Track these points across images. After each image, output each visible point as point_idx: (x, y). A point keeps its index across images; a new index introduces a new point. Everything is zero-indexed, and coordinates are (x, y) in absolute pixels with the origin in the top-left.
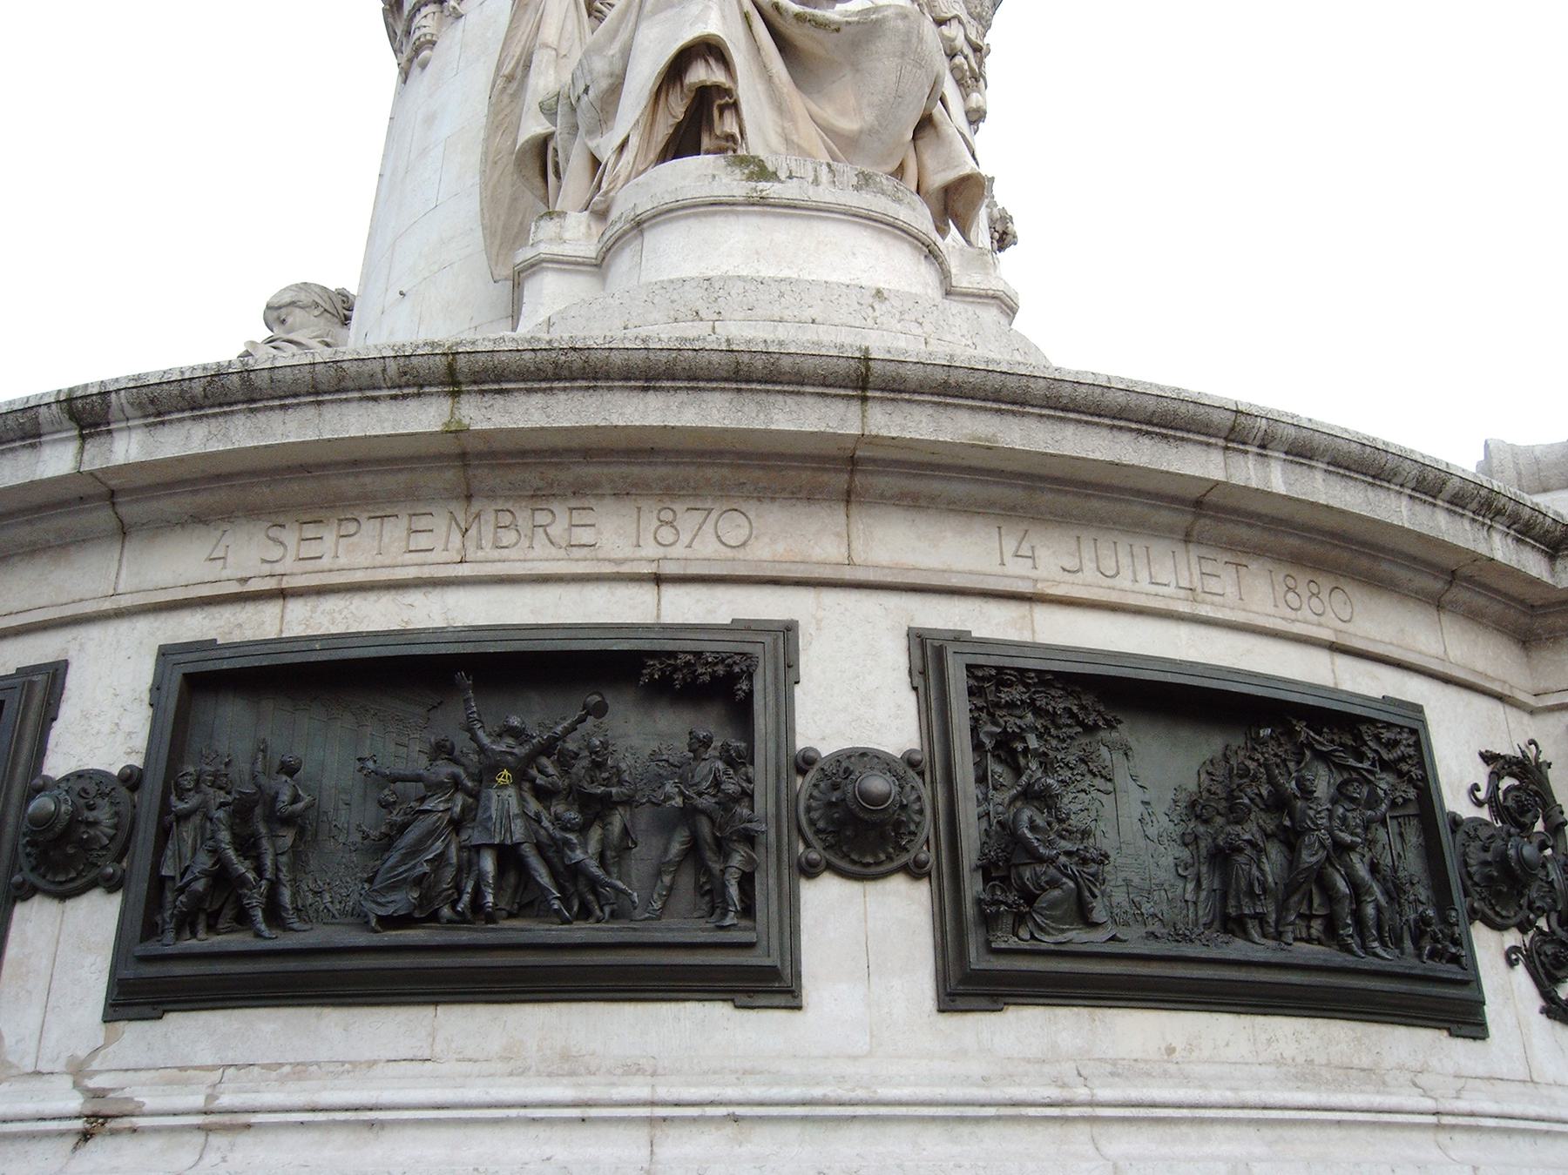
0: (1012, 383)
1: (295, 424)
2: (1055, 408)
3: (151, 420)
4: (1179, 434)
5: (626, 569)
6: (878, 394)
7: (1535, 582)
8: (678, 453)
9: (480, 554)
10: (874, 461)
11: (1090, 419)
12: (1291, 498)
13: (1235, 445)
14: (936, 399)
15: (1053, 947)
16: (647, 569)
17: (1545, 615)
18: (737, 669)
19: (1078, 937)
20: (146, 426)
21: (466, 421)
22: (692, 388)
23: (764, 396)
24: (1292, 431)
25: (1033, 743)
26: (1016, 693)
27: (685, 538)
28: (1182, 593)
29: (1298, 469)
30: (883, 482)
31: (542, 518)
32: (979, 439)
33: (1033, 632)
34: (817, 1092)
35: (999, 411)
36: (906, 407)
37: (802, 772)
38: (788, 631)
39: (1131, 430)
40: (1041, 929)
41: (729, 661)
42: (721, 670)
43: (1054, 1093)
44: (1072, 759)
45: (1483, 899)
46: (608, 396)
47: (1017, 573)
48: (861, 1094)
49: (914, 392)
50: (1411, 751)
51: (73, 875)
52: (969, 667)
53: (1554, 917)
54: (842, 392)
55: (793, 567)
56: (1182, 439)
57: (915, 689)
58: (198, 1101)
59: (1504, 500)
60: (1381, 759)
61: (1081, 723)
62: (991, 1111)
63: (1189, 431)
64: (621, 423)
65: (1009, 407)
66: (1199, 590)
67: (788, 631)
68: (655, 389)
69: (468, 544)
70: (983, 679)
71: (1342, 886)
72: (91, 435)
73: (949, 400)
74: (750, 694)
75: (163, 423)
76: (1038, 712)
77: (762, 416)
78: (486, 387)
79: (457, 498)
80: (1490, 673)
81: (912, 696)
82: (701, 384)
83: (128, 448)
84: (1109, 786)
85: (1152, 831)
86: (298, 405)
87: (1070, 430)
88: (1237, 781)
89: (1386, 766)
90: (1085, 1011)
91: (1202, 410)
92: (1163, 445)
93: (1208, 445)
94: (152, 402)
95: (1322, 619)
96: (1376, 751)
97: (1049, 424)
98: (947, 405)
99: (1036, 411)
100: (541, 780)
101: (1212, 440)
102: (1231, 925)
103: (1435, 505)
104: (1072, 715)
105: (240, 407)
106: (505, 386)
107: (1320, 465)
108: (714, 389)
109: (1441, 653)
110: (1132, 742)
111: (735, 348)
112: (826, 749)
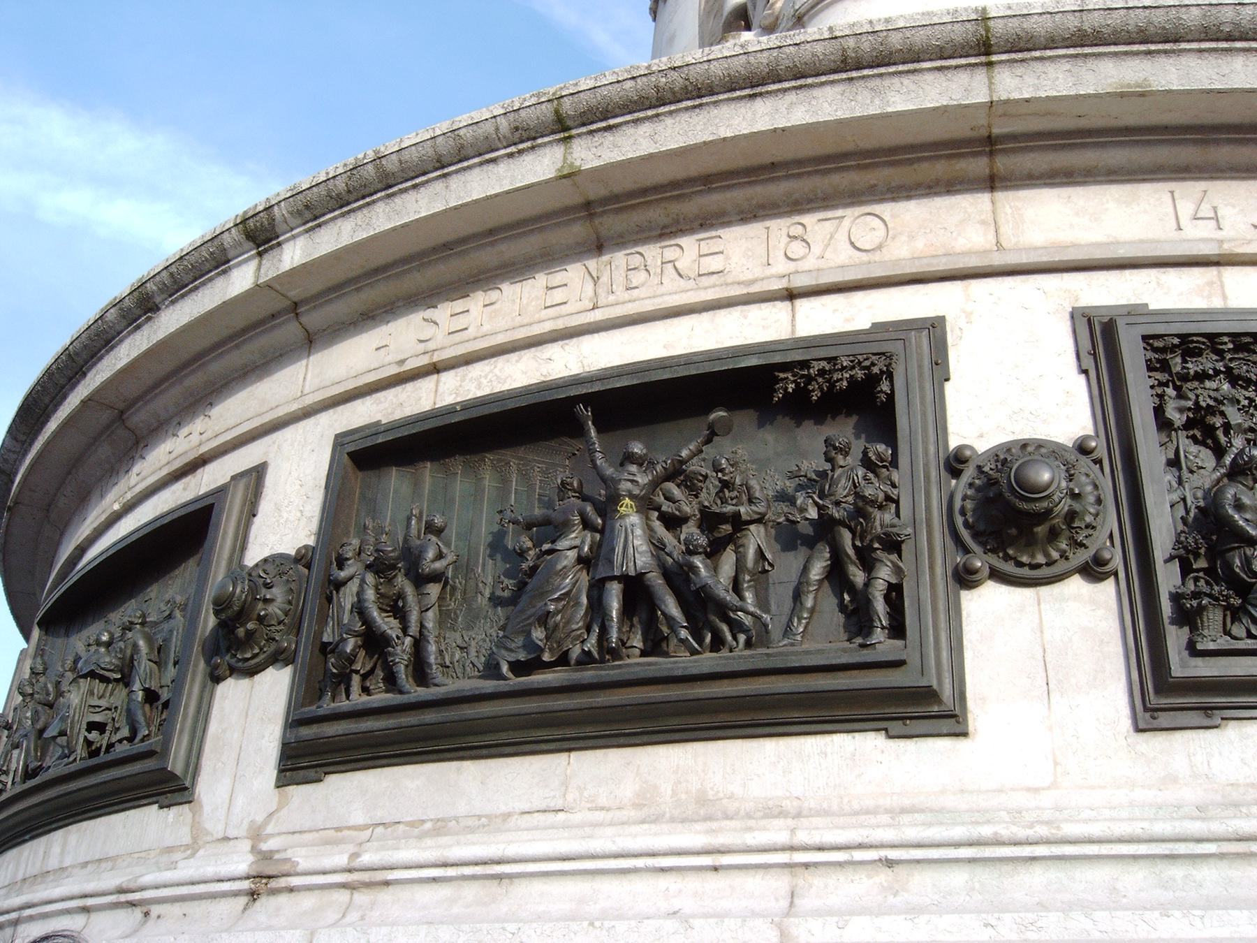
0: (1159, 18)
1: (426, 200)
2: (1218, 40)
3: (310, 224)
6: (1004, 57)
8: (799, 163)
9: (612, 298)
10: (1014, 137)
14: (1072, 51)
18: (876, 370)
20: (307, 231)
21: (577, 163)
22: (800, 87)
23: (878, 81)
26: (1208, 362)
27: (816, 249)
31: (670, 254)
32: (1129, 85)
33: (1225, 297)
35: (1149, 53)
36: (1038, 66)
37: (956, 473)
38: (934, 328)
41: (867, 363)
42: (859, 374)
46: (715, 111)
47: (1199, 237)
48: (1043, 831)
49: (1045, 48)
51: (256, 651)
52: (1145, 338)
54: (963, 61)
55: (935, 261)
57: (1085, 372)
58: (341, 860)
64: (729, 134)
65: (1160, 47)
67: (934, 328)
68: (761, 94)
69: (600, 291)
70: (1163, 350)
72: (266, 251)
73: (1087, 50)
74: (891, 397)
75: (319, 226)
77: (877, 102)
78: (594, 127)
79: (589, 251)
82: (810, 81)
83: (294, 253)
86: (427, 182)
94: (307, 207)
97: (1212, 59)
98: (1086, 55)
99: (1194, 45)
100: (667, 507)
105: (379, 195)
106: (612, 122)
108: (822, 84)
111: (838, 34)
112: (982, 446)
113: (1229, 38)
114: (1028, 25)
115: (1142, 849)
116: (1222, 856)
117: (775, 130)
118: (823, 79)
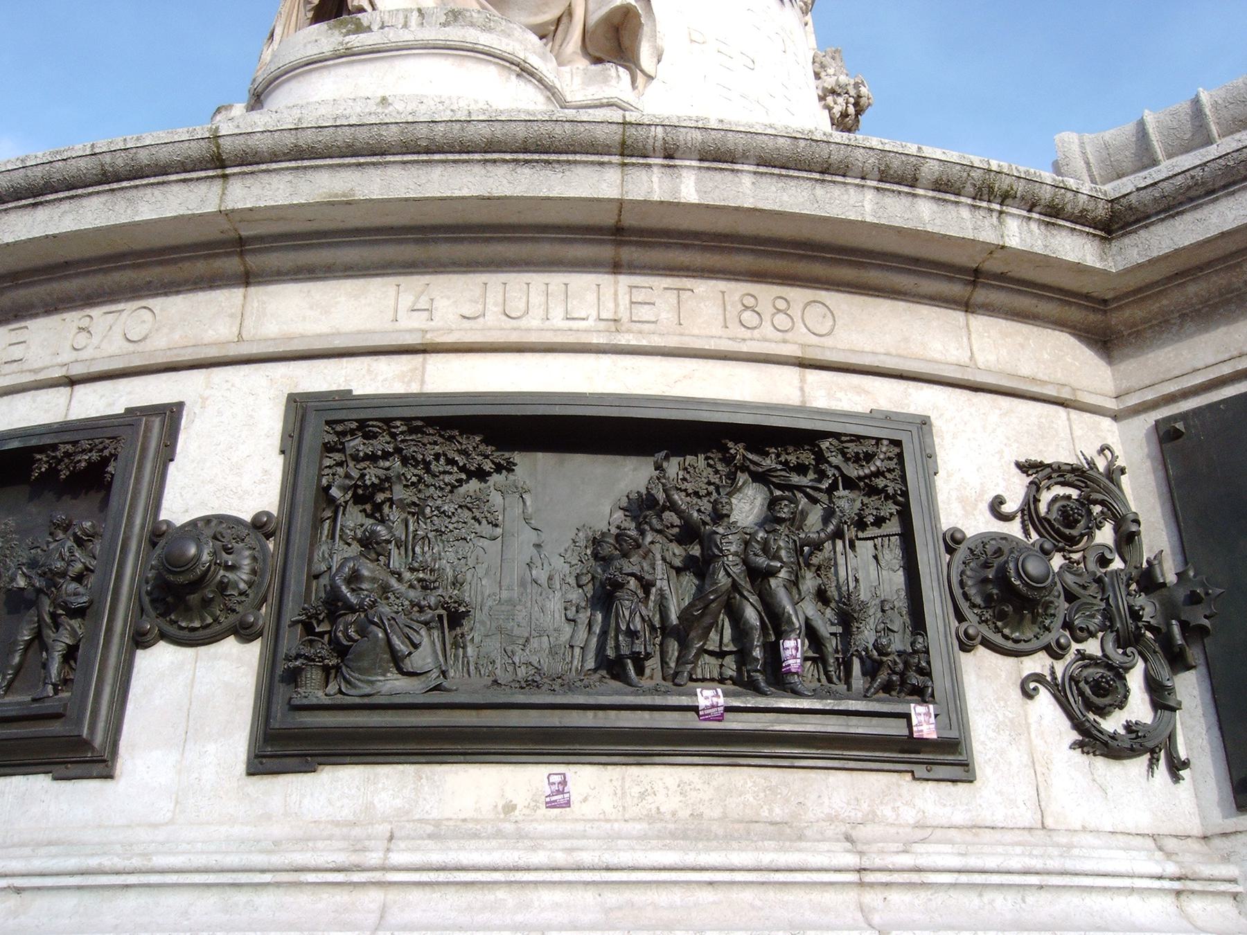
0: (362, 134)
2: (419, 153)
4: (563, 157)
5: (42, 376)
7: (1079, 269)
10: (260, 239)
11: (457, 157)
12: (707, 206)
13: (634, 160)
14: (293, 164)
16: (57, 373)
17: (1120, 308)
18: (106, 453)
22: (72, 197)
23: (134, 192)
24: (698, 135)
25: (399, 492)
28: (602, 325)
29: (718, 176)
30: (273, 260)
32: (336, 195)
33: (423, 382)
34: (93, 862)
36: (265, 178)
38: (171, 415)
39: (505, 161)
43: (341, 858)
47: (410, 328)
48: (136, 862)
49: (271, 162)
50: (892, 464)
52: (328, 423)
53: (1111, 637)
54: (203, 174)
55: (183, 352)
56: (568, 162)
59: (1008, 180)
60: (842, 474)
62: (267, 878)
63: (575, 153)
64: (11, 240)
65: (369, 159)
66: (625, 319)
67: (171, 415)
68: (41, 203)
70: (342, 434)
71: (751, 615)
73: (306, 163)
80: (1040, 376)
81: (280, 460)
82: (80, 191)
85: (541, 575)
87: (437, 172)
89: (850, 484)
91: (581, 128)
92: (548, 172)
93: (601, 164)
95: (788, 336)
96: (837, 468)
97: (414, 170)
98: (305, 168)
101: (606, 159)
103: (915, 195)
104: (452, 462)
107: (746, 167)
108: (90, 194)
109: (964, 358)
111: (97, 151)
113: (428, 151)
114: (253, 142)
115: (212, 878)
116: (278, 885)
117: (47, 236)
118: (90, 190)
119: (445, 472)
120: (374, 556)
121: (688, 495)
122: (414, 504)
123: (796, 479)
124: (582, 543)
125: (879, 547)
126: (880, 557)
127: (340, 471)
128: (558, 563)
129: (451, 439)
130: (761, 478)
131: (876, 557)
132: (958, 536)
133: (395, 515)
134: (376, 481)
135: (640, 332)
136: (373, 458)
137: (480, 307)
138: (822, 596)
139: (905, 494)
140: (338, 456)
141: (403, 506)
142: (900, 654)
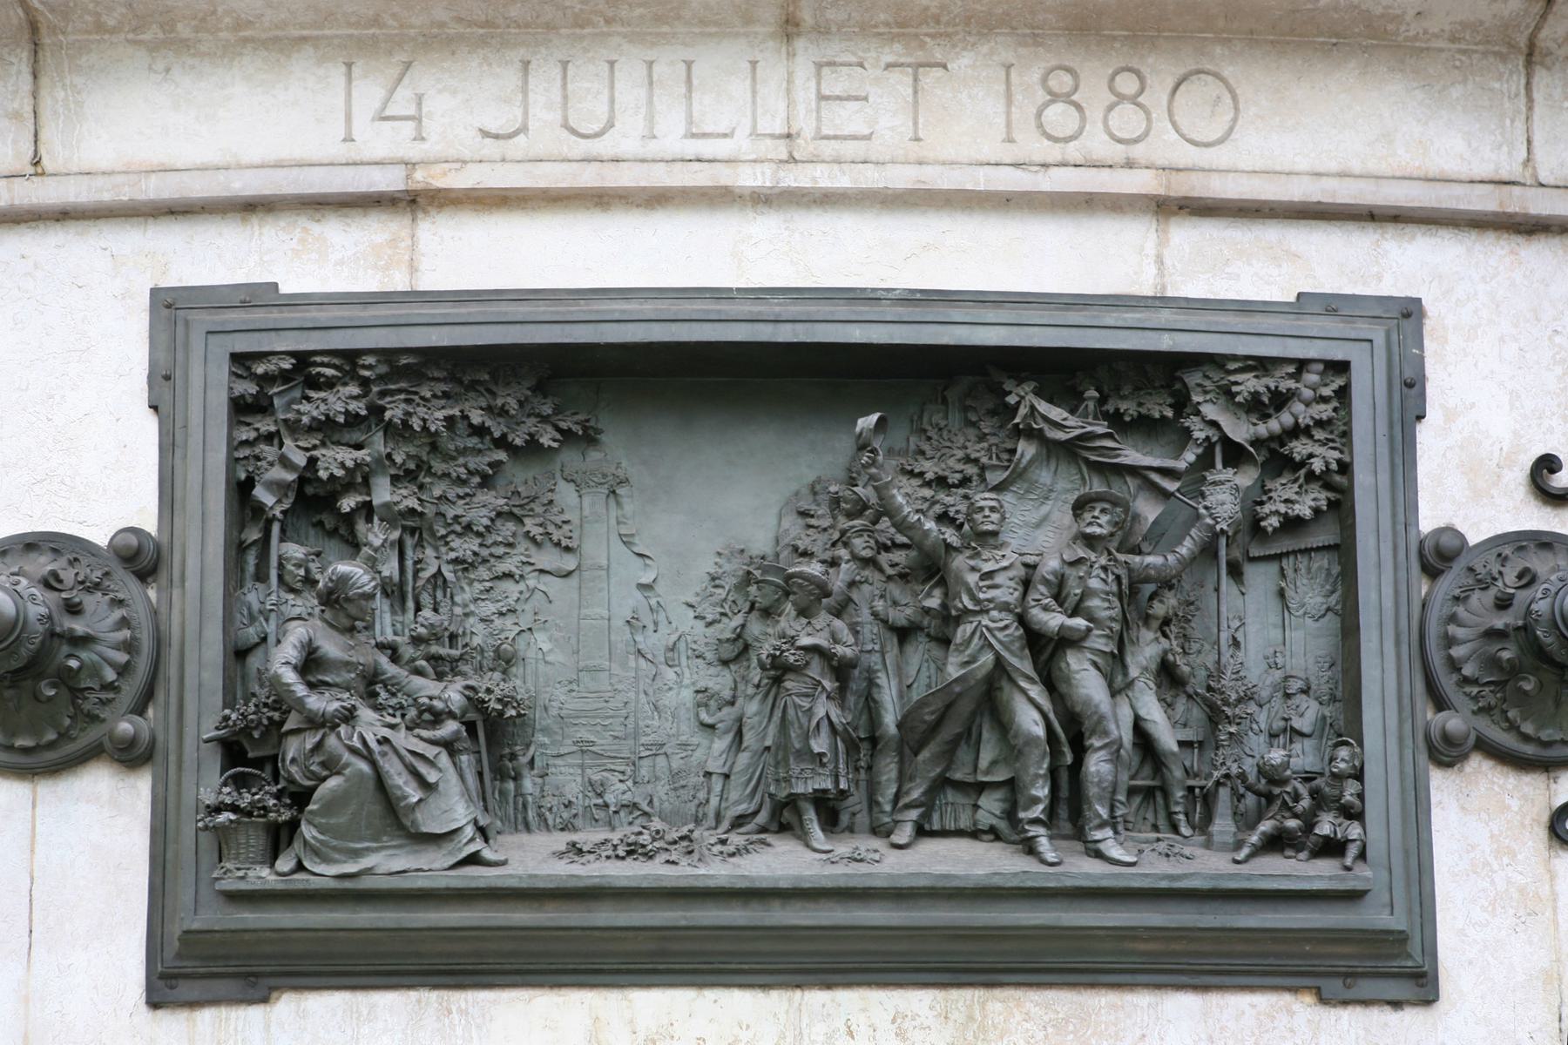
15: (333, 884)
19: (388, 863)
26: (341, 401)
33: (413, 269)
40: (316, 852)
44: (480, 517)
45: (1486, 710)
60: (1226, 441)
61: (502, 443)
71: (1030, 721)
76: (399, 432)
84: (569, 563)
85: (654, 642)
88: (844, 523)
89: (1235, 455)
90: (432, 997)
96: (1214, 424)
102: (787, 815)
104: (480, 431)
110: (629, 467)
119: (464, 452)
120: (346, 622)
121: (928, 484)
122: (412, 511)
123: (1132, 456)
124: (729, 582)
125: (1289, 572)
126: (1289, 593)
127: (269, 451)
128: (686, 622)
129: (473, 386)
130: (1071, 451)
131: (1281, 594)
132: (1447, 542)
133: (375, 535)
134: (339, 473)
135: (838, 161)
136: (326, 429)
137: (519, 112)
138: (1168, 676)
139: (1345, 468)
140: (266, 425)
141: (392, 516)
142: (1308, 779)
